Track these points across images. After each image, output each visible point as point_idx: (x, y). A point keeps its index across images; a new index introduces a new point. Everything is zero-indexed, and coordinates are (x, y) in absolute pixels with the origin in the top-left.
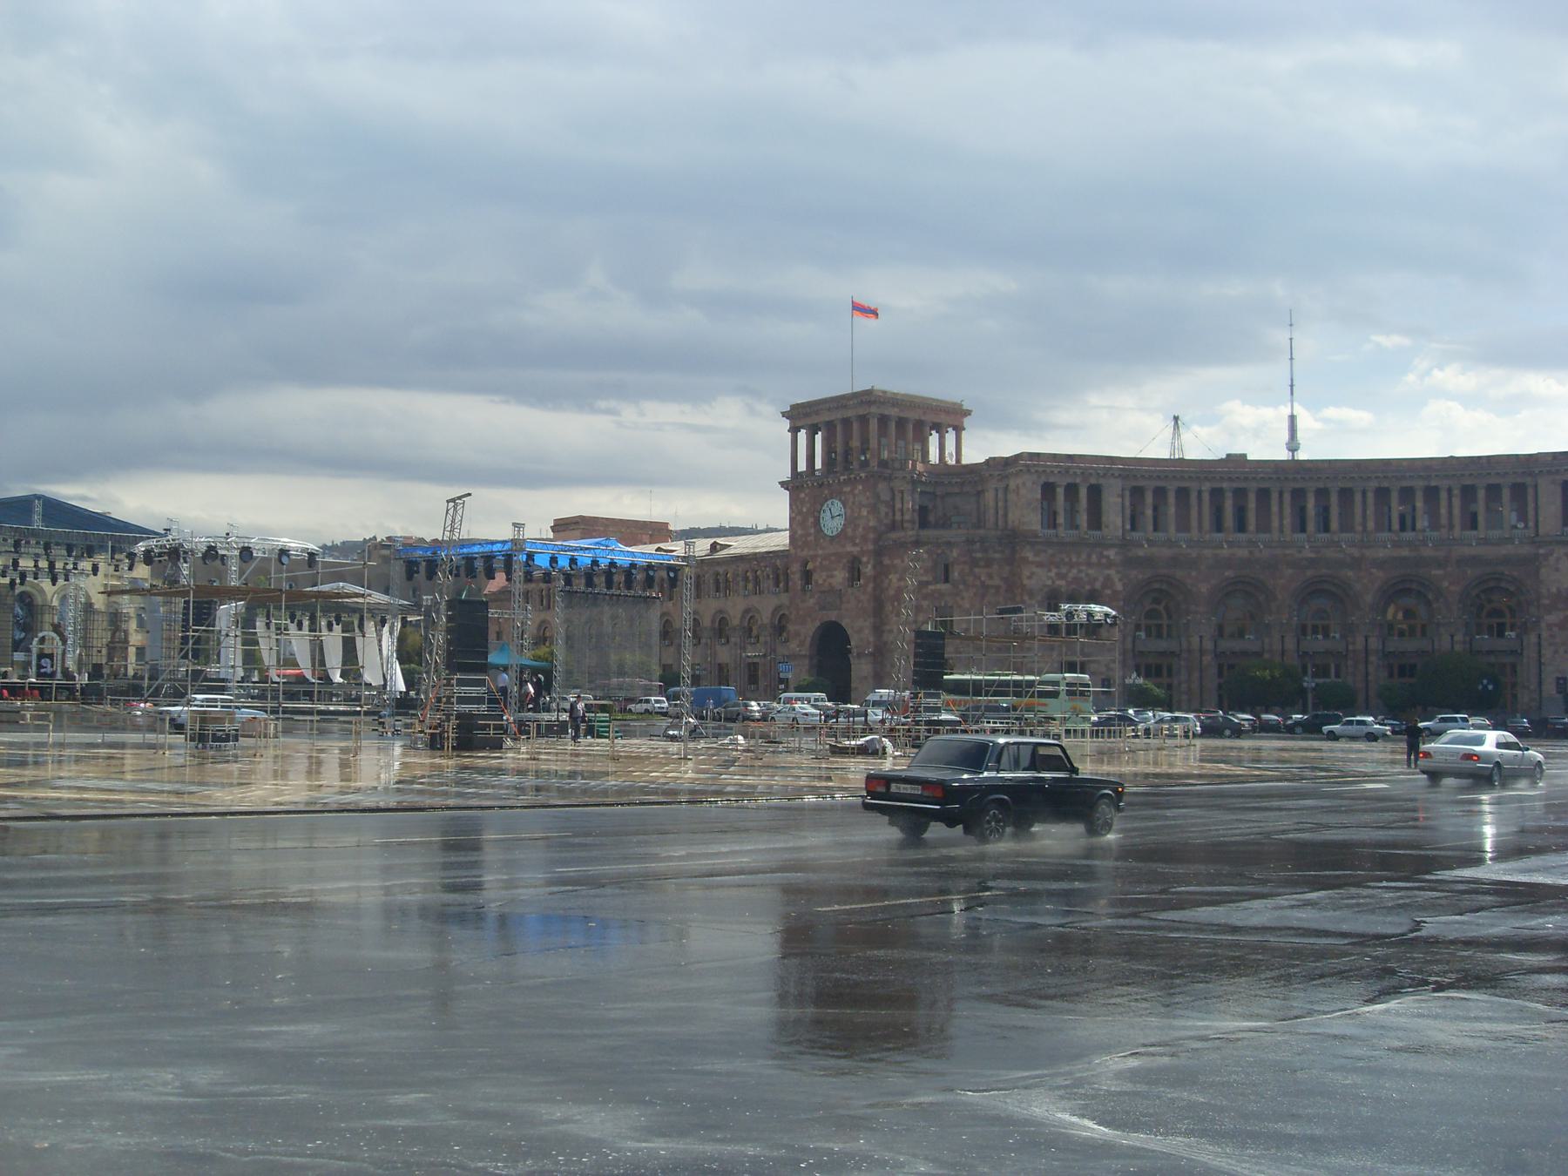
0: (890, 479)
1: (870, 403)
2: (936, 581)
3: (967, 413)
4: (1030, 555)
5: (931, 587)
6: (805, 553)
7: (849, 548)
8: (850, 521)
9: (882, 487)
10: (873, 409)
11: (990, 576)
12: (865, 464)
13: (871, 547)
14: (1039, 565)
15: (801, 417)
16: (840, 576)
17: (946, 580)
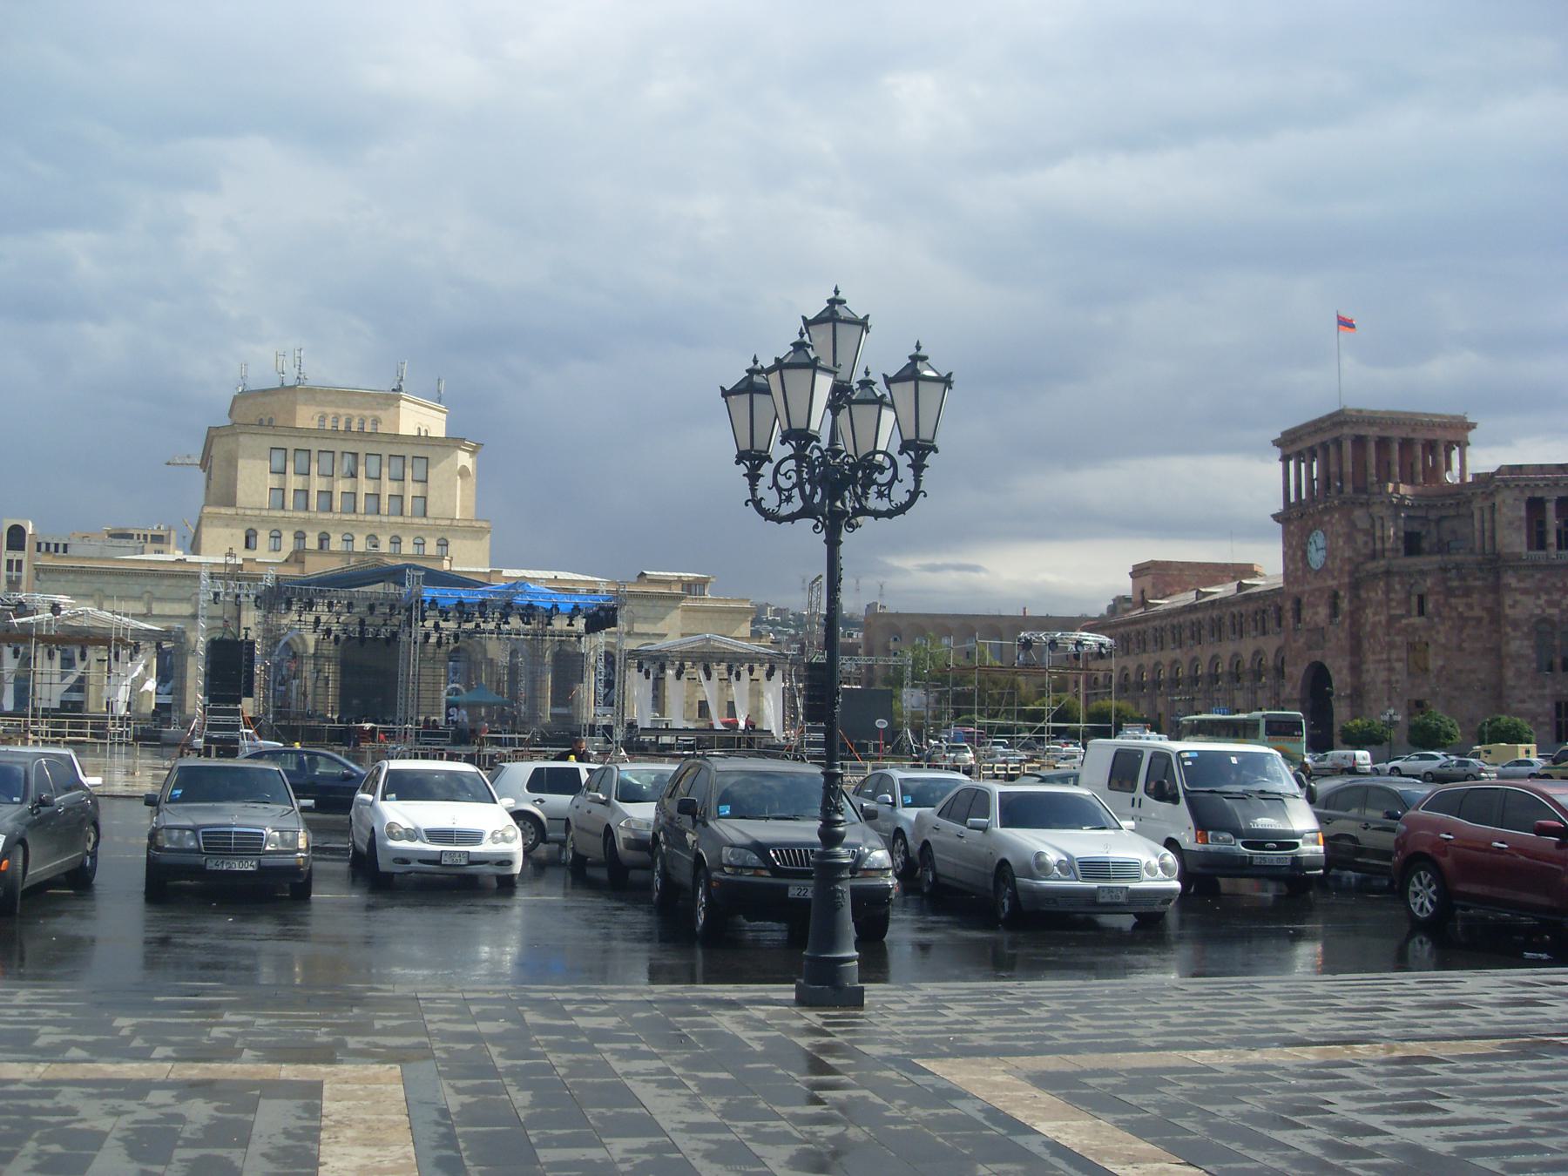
0: (1366, 505)
1: (1342, 424)
2: (1409, 614)
3: (1472, 426)
4: (1513, 582)
5: (1404, 621)
6: (1295, 589)
7: (1331, 583)
8: (1330, 553)
9: (1358, 513)
10: (1346, 431)
11: (1470, 607)
12: (1341, 491)
13: (1346, 580)
14: (1525, 592)
15: (1293, 445)
16: (1323, 611)
17: (1421, 612)
